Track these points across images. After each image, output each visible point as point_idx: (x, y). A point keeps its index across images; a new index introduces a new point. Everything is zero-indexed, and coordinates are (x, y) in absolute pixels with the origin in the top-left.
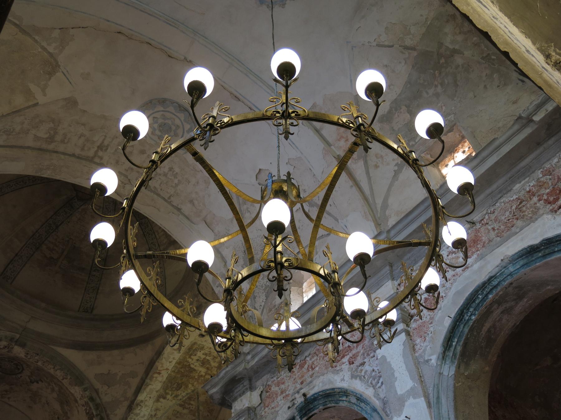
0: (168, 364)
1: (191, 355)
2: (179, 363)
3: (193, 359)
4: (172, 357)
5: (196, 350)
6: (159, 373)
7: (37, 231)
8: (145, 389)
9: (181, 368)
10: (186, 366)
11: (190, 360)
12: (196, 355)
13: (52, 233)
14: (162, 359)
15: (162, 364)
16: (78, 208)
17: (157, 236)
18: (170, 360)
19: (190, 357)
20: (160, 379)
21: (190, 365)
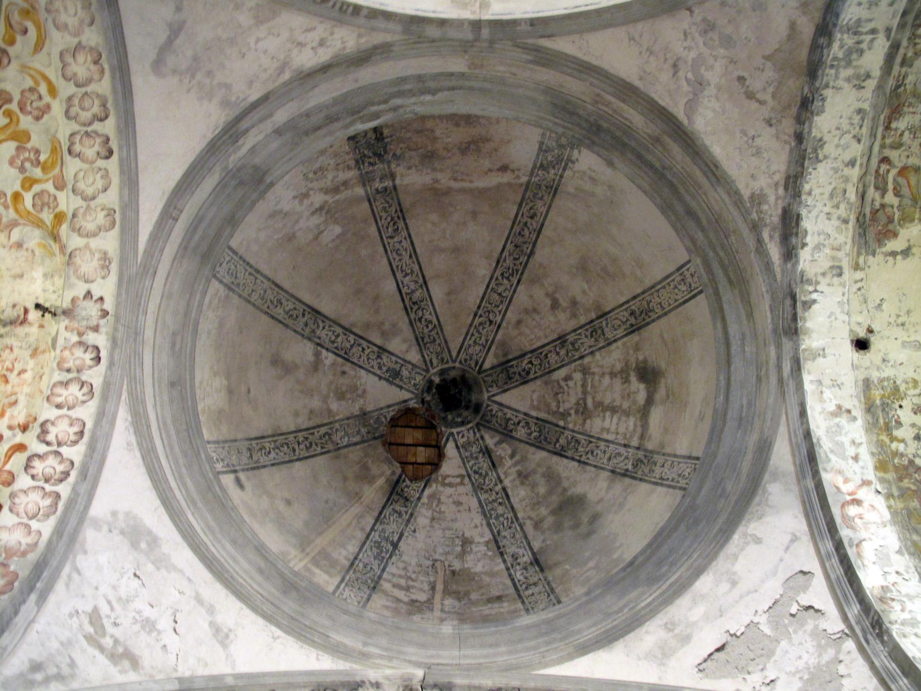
0: (856, 467)
1: (888, 429)
2: (881, 466)
3: (903, 441)
4: (846, 441)
5: (885, 406)
6: (858, 502)
7: (356, 558)
8: (859, 555)
9: (900, 479)
10: (906, 468)
11: (901, 447)
12: (899, 424)
13: (391, 557)
14: (829, 460)
15: (840, 472)
16: (419, 498)
17: (610, 437)
18: (851, 451)
19: (893, 439)
20: (871, 516)
21: (911, 462)
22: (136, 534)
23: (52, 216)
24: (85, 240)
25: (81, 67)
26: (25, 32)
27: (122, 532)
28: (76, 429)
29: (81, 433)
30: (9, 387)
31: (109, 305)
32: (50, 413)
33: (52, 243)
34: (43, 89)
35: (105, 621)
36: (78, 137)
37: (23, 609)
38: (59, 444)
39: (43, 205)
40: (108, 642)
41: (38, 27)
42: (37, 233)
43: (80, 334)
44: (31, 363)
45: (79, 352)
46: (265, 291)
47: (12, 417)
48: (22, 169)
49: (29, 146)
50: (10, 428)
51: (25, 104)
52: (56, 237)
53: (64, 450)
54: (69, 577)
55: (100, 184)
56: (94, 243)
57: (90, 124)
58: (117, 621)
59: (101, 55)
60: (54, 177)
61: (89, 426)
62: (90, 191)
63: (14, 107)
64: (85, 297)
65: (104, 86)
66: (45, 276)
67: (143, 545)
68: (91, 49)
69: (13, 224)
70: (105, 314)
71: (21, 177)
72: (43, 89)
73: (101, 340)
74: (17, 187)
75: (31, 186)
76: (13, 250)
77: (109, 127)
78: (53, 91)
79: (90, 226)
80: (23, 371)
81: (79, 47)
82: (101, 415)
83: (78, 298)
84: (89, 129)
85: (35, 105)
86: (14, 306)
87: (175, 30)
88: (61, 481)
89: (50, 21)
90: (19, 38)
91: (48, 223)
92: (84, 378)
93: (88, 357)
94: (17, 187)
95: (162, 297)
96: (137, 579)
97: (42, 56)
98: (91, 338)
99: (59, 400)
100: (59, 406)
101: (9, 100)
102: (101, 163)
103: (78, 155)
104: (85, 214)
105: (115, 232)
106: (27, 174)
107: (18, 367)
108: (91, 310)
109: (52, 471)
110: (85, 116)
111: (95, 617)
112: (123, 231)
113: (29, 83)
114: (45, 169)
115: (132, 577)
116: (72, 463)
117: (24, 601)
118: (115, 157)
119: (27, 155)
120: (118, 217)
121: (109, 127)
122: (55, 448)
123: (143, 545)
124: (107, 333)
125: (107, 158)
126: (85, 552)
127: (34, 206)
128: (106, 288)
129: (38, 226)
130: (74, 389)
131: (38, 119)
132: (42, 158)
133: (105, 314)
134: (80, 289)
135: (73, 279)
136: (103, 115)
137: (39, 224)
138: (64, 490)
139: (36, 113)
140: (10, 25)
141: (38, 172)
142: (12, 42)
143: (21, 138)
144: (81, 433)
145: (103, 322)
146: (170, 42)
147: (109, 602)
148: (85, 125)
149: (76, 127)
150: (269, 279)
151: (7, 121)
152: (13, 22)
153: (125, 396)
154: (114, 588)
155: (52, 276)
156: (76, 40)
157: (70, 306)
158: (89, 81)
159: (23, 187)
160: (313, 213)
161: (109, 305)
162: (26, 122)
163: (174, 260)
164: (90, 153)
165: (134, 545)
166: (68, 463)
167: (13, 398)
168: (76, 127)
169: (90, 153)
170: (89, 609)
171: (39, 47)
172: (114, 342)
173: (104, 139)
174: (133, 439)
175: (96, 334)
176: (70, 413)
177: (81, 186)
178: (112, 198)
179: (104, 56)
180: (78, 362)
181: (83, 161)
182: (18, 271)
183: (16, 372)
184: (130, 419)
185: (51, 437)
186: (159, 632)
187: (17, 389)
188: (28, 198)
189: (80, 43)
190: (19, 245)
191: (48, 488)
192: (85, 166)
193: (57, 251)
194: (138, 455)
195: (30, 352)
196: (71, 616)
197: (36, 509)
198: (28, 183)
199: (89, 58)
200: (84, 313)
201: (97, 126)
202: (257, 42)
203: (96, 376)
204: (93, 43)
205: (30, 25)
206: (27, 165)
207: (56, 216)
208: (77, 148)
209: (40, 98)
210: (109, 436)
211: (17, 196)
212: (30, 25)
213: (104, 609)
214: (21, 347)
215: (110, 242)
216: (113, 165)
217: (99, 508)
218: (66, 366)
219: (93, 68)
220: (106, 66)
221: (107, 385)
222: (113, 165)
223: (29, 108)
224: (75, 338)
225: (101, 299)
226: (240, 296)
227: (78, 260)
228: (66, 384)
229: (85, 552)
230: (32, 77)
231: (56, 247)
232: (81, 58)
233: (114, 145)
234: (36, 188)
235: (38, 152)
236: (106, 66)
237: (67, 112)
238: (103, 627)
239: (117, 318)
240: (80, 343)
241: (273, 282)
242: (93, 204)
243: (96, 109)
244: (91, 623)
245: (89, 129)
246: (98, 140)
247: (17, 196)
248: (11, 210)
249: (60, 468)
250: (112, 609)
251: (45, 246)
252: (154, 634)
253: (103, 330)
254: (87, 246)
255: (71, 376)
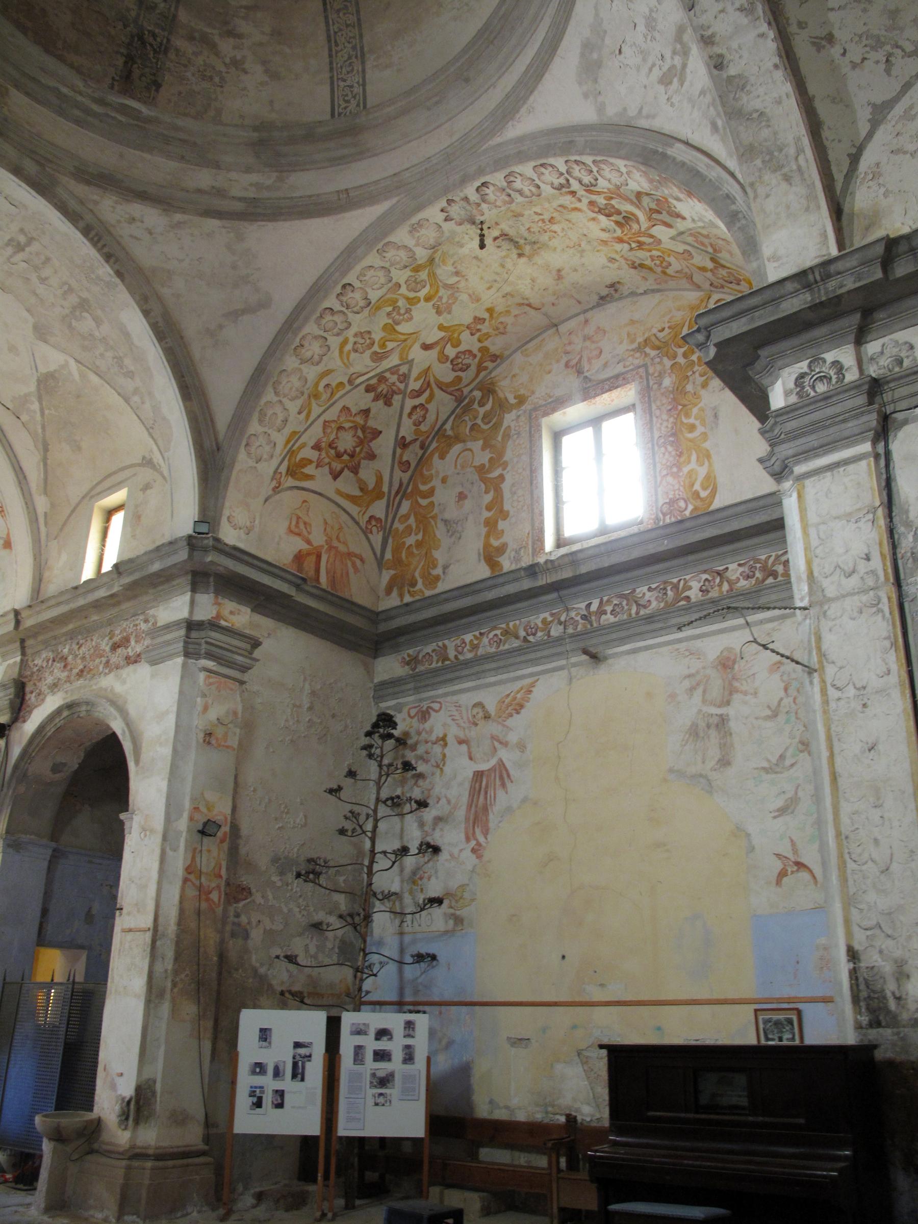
22: (591, 69)
23: (420, 273)
24: (414, 249)
25: (315, 348)
26: (327, 385)
27: (595, 81)
28: (543, 170)
29: (542, 165)
30: (554, 215)
31: (443, 203)
32: (547, 190)
33: (437, 260)
34: (349, 347)
35: (665, 69)
36: (355, 309)
37: (679, 158)
38: (562, 174)
39: (417, 283)
40: (678, 61)
41: (317, 385)
42: (439, 272)
43: (478, 205)
44: (527, 213)
45: (491, 197)
46: (338, 11)
47: (571, 203)
48: (408, 311)
49: (390, 321)
50: (580, 200)
51: (368, 345)
52: (431, 260)
53: (563, 169)
54: (648, 117)
55: (371, 272)
56: (411, 243)
57: (341, 312)
58: (660, 57)
59: (295, 349)
60: (394, 293)
61: (533, 164)
62: (381, 273)
63: (376, 348)
64: (452, 220)
65: (311, 328)
66: (462, 246)
67: (595, 56)
68: (297, 356)
69: (446, 286)
70: (450, 202)
71: (413, 307)
72: (349, 347)
73: (470, 191)
74: (422, 303)
75: (413, 299)
76: (463, 274)
77: (331, 302)
78: (346, 341)
79: (403, 254)
80: (536, 213)
81: (303, 361)
82: (522, 157)
83: (456, 223)
84: (344, 309)
85: (363, 341)
86: (499, 247)
87: (234, 315)
88: (584, 163)
89: (307, 386)
90: (334, 384)
91: (427, 271)
92: (505, 184)
93: (489, 191)
94: (422, 303)
95: (409, 142)
96: (623, 50)
97: (330, 366)
98: (474, 197)
99: (533, 189)
100: (538, 187)
101: (376, 353)
102: (357, 284)
103: (366, 298)
104: (398, 263)
105: (391, 238)
106: (408, 306)
107: (537, 218)
108: (456, 210)
109: (582, 171)
110: (338, 318)
111: (665, 80)
112: (386, 235)
113: (353, 355)
114: (396, 301)
115: (623, 56)
116: (566, 162)
117: (674, 159)
118: (345, 281)
119: (397, 317)
120: (380, 246)
121: (331, 302)
122: (566, 175)
123: (595, 56)
124: (462, 191)
125: (350, 284)
126: (625, 109)
127: (424, 287)
128: (433, 213)
129: (434, 274)
130: (518, 184)
131: (369, 332)
132: (390, 309)
133: (450, 202)
134: (447, 226)
135: (447, 234)
136: (327, 311)
137: (432, 275)
138: (588, 160)
139: (367, 336)
140: (332, 394)
141: (401, 303)
142: (341, 384)
143: (389, 329)
144: (542, 165)
145: (457, 199)
146: (244, 311)
147: (650, 70)
148: (344, 313)
149: (350, 315)
150: (326, 17)
151: (387, 343)
152: (329, 395)
153: (497, 140)
154: (638, 69)
155: (458, 242)
156: (302, 367)
157: (466, 223)
158: (316, 337)
159: (419, 301)
160: (240, 36)
161: (443, 203)
162: (377, 336)
163: (376, 155)
164: (358, 295)
165: (599, 64)
166: (569, 164)
167: (559, 209)
168: (350, 315)
169: (358, 295)
170: (662, 88)
171: (328, 373)
172: (465, 180)
173: (341, 298)
174: (523, 110)
175: (469, 197)
176: (536, 179)
177: (383, 280)
178: (373, 259)
179: (293, 347)
180: (498, 194)
181: (367, 293)
182: (474, 261)
183: (541, 217)
184: (510, 123)
185: (562, 181)
186: (651, 11)
187: (552, 210)
188: (422, 293)
189: (301, 363)
190: (457, 273)
191: (595, 169)
192: (369, 290)
193: (439, 253)
194: (532, 98)
195: (521, 218)
196: (672, 105)
197: (614, 172)
198: (413, 301)
199: (303, 351)
200: (463, 213)
201: (337, 307)
202: (183, 260)
203: (498, 178)
204: (294, 358)
205: (321, 388)
206: (402, 311)
207: (418, 271)
208: (362, 303)
209: (355, 343)
210: (532, 136)
211: (428, 299)
212: (321, 388)
213: (656, 73)
214: (523, 225)
215: (402, 236)
216: (351, 278)
217: (585, 113)
218: (507, 199)
219: (306, 344)
220: (298, 340)
221: (498, 165)
222: (351, 278)
223: (368, 341)
224: (484, 206)
225: (442, 211)
226: (361, 36)
227: (432, 242)
228: (520, 192)
229: (625, 109)
230: (348, 359)
231: (437, 256)
232: (309, 354)
233: (338, 289)
234: (412, 295)
235: (389, 314)
236: (298, 340)
237: (347, 329)
238: (669, 70)
239: (446, 190)
240: (484, 201)
241: (325, 10)
242: (387, 265)
243: (328, 317)
244: (671, 83)
245: (344, 309)
246: (344, 299)
247: (428, 299)
248: (440, 294)
249: (577, 168)
250: (654, 65)
251: (444, 261)
252: (654, 15)
253: (462, 195)
254: (417, 245)
255: (511, 192)
